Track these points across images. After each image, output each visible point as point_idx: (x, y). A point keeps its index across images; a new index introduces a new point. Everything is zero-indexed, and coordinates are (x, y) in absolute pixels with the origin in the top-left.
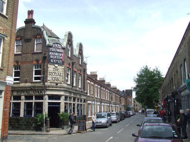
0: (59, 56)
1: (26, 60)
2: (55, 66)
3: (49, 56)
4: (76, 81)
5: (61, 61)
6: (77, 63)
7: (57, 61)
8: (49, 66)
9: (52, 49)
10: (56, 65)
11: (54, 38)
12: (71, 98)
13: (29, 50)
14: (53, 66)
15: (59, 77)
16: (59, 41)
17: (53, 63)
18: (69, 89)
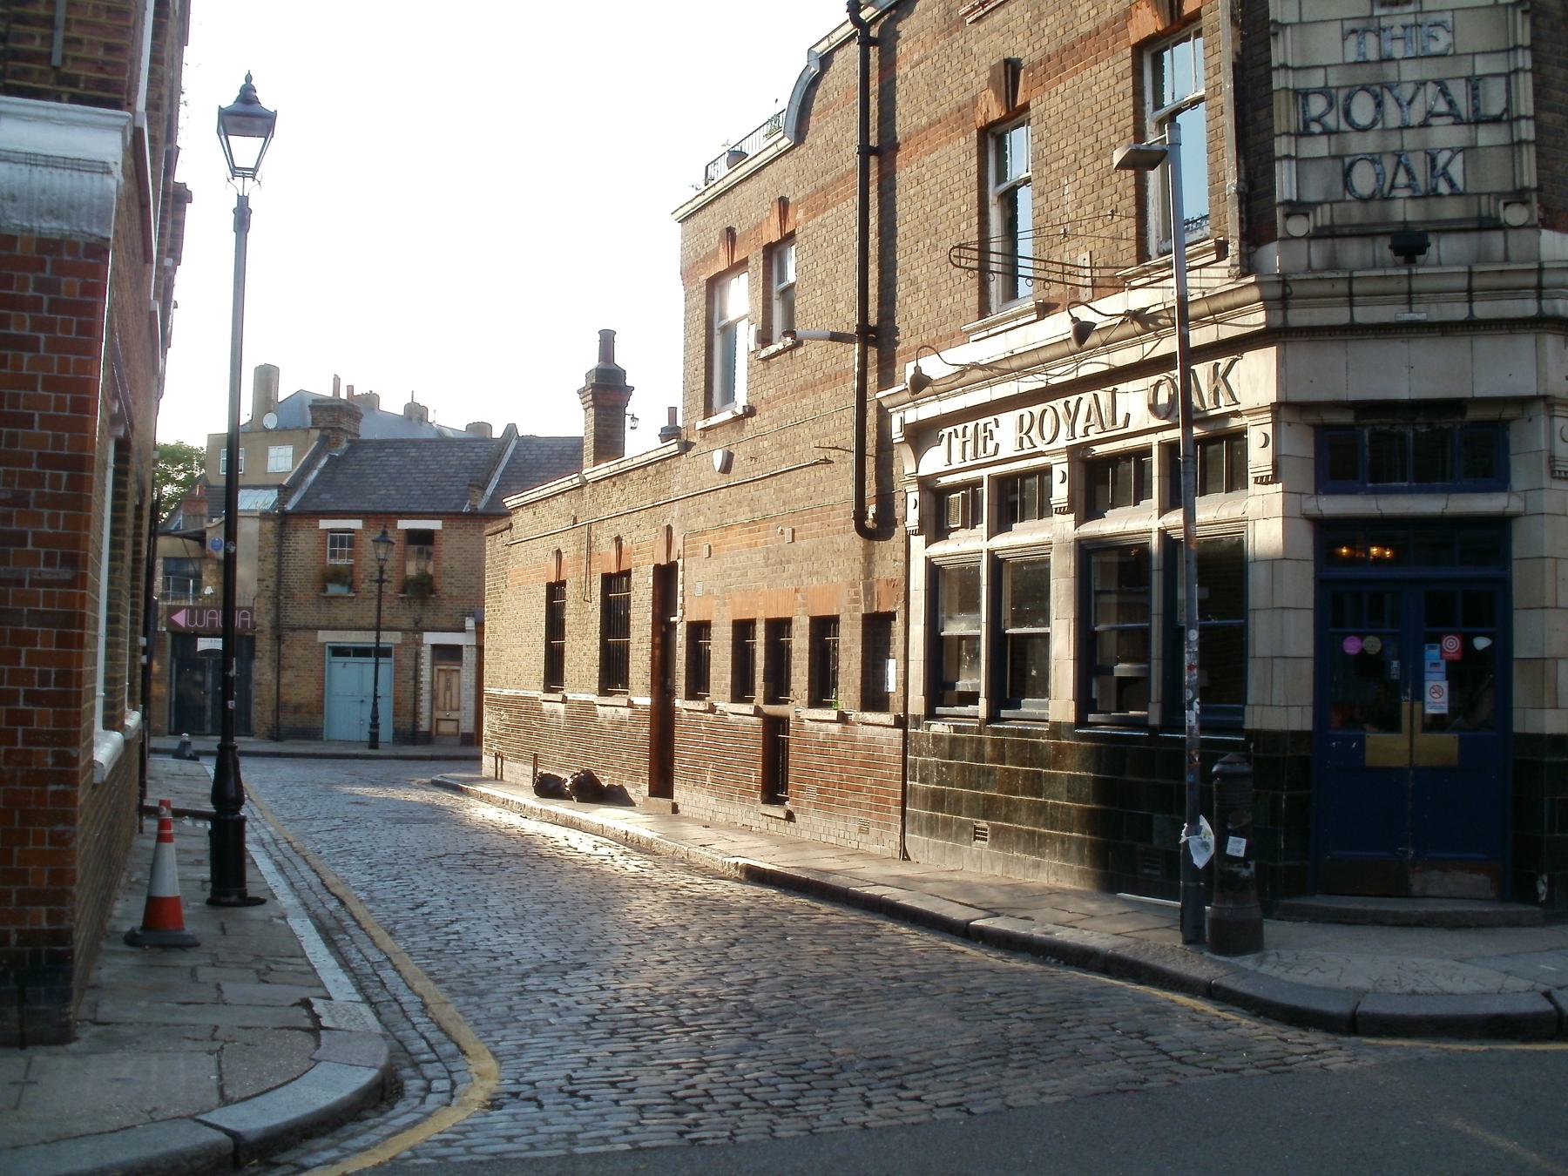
15: (1445, 135)
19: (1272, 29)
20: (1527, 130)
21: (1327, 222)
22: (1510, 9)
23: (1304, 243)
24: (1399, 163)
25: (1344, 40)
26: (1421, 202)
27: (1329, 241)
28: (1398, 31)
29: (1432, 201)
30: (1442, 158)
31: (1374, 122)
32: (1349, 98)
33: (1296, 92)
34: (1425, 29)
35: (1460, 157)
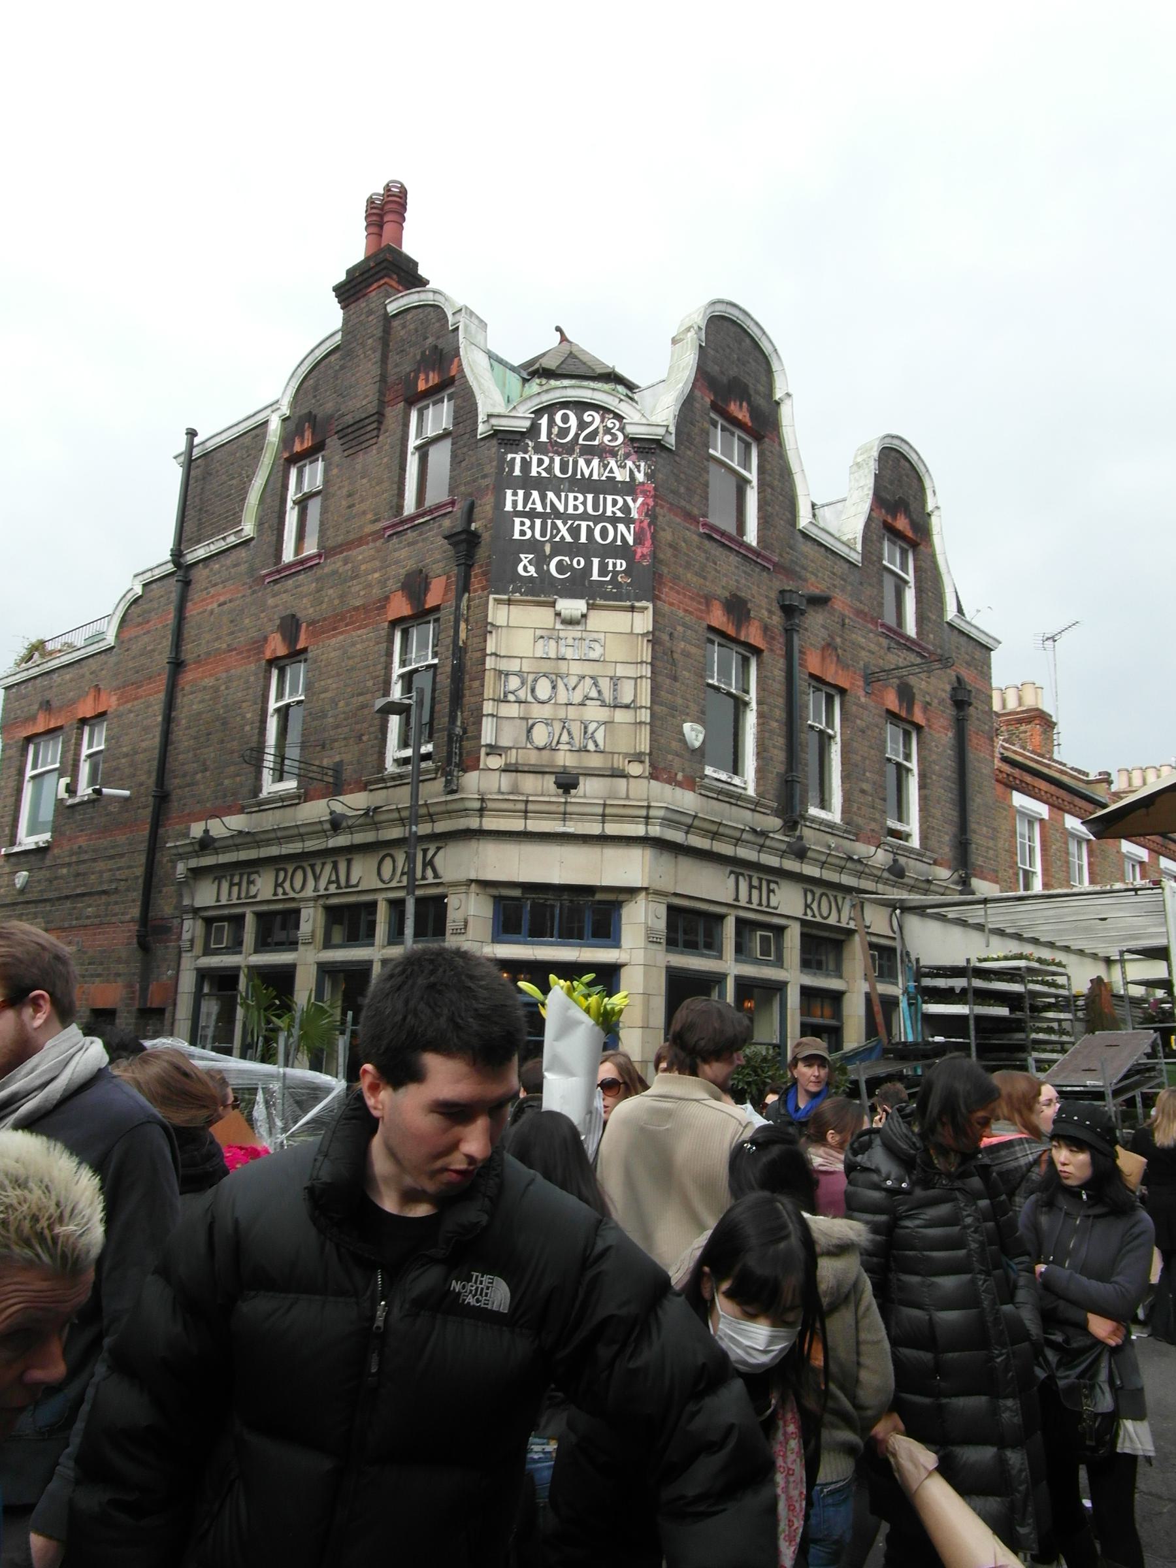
0: (602, 518)
2: (558, 614)
3: (503, 521)
5: (621, 565)
7: (579, 563)
8: (498, 614)
9: (526, 465)
10: (573, 606)
12: (780, 930)
13: (364, 513)
14: (541, 617)
15: (594, 713)
18: (673, 819)
19: (489, 628)
20: (645, 716)
21: (513, 761)
22: (640, 637)
23: (497, 773)
24: (564, 727)
25: (535, 642)
26: (575, 753)
27: (514, 774)
29: (583, 754)
31: (550, 699)
32: (535, 680)
34: (587, 642)
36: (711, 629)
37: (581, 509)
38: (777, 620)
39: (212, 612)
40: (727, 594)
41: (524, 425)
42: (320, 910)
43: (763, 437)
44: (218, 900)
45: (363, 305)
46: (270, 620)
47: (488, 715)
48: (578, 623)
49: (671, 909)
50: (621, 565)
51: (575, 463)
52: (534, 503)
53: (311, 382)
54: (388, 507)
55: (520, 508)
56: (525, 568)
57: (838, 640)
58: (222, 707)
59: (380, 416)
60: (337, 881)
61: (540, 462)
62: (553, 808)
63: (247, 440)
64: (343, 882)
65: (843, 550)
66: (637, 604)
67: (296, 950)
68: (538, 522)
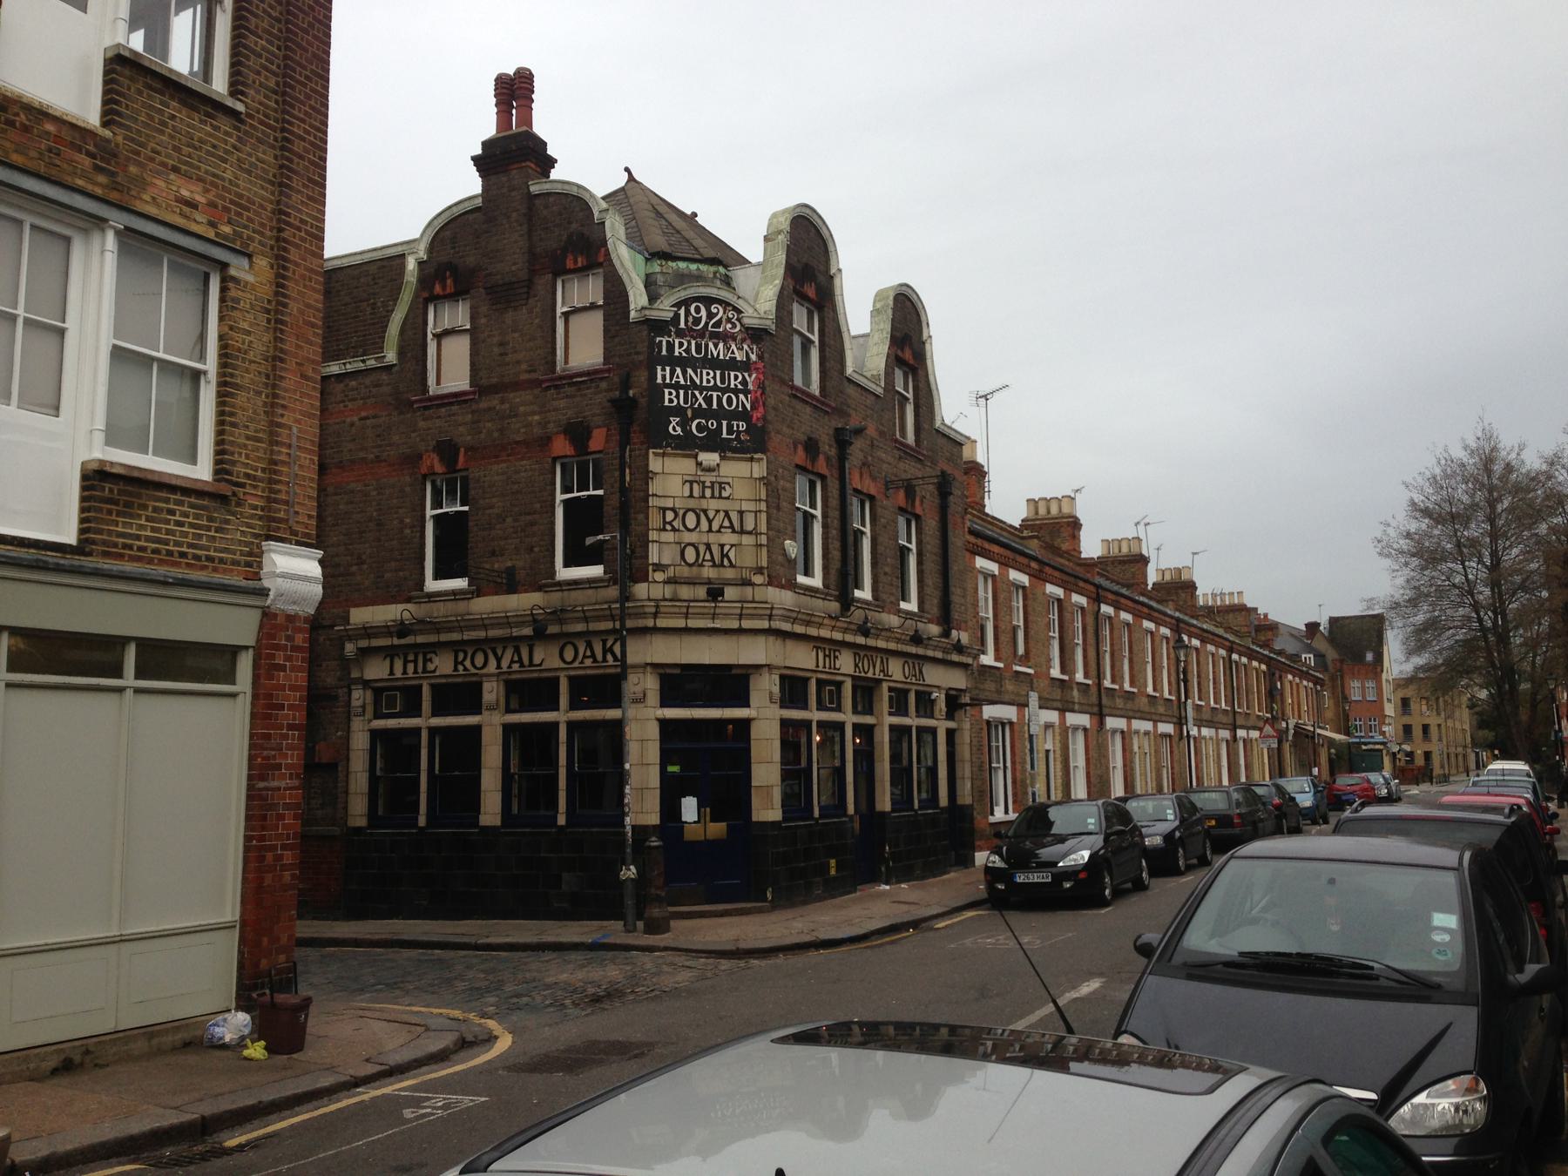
1: (501, 430)
2: (699, 464)
3: (656, 391)
4: (874, 564)
5: (743, 426)
6: (882, 434)
8: (655, 464)
9: (670, 346)
11: (693, 267)
12: (839, 685)
13: (518, 362)
14: (685, 466)
15: (728, 538)
16: (727, 282)
17: (687, 445)
19: (650, 475)
20: (764, 540)
23: (662, 585)
26: (716, 569)
27: (673, 585)
28: (709, 484)
29: (721, 569)
30: (726, 548)
31: (696, 528)
33: (660, 508)
35: (734, 548)
36: (797, 466)
37: (712, 383)
38: (833, 452)
39: (352, 425)
40: (806, 438)
41: (668, 315)
42: (502, 683)
43: (824, 307)
44: (392, 673)
45: (504, 179)
46: (423, 440)
47: (653, 541)
48: (714, 470)
49: (782, 677)
50: (743, 426)
51: (707, 346)
52: (678, 377)
53: (448, 233)
54: (543, 362)
55: (668, 381)
56: (674, 429)
57: (870, 458)
58: (376, 511)
59: (530, 284)
60: (520, 661)
61: (681, 345)
62: (706, 611)
63: (373, 269)
64: (526, 661)
65: (872, 386)
66: (756, 456)
67: (481, 713)
68: (682, 392)
